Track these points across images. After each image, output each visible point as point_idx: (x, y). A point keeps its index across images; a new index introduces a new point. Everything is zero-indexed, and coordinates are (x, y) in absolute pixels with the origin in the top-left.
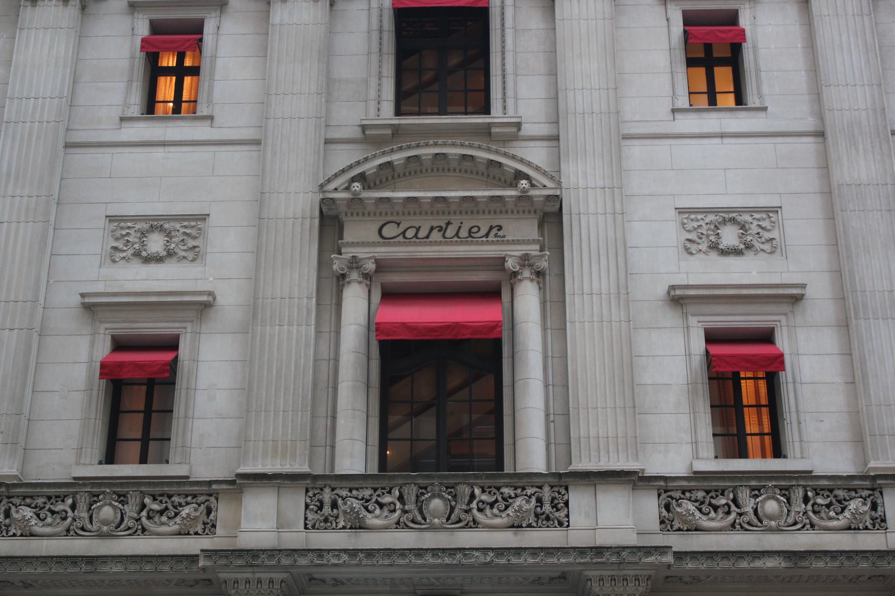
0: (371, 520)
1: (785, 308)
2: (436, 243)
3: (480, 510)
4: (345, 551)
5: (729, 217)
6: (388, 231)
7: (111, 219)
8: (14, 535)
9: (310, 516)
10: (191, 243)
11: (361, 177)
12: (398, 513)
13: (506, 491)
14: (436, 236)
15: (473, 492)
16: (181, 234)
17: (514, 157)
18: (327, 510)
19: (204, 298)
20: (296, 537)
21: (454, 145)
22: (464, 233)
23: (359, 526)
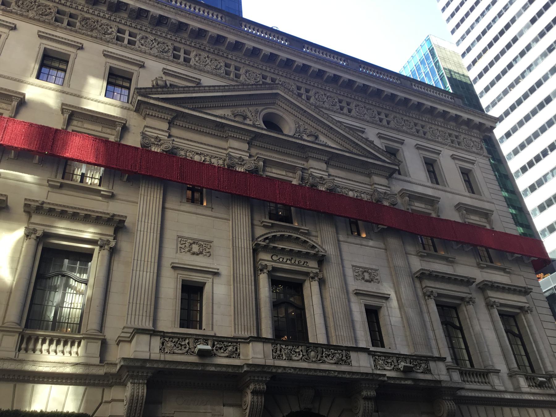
0: (294, 358)
1: (384, 301)
2: (288, 264)
3: (326, 357)
4: (293, 368)
5: (366, 270)
6: (275, 258)
7: (179, 237)
8: (167, 353)
9: (274, 354)
10: (208, 250)
11: (267, 238)
12: (301, 356)
13: (333, 351)
14: (288, 262)
15: (323, 351)
16: (205, 248)
17: (312, 241)
18: (278, 352)
19: (216, 271)
20: (270, 362)
21: (287, 232)
22: (297, 263)
23: (290, 359)
